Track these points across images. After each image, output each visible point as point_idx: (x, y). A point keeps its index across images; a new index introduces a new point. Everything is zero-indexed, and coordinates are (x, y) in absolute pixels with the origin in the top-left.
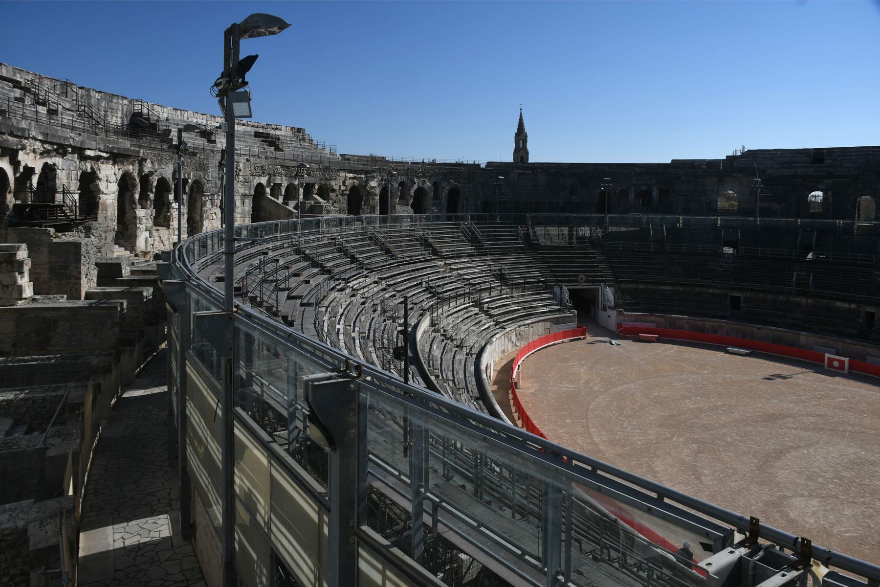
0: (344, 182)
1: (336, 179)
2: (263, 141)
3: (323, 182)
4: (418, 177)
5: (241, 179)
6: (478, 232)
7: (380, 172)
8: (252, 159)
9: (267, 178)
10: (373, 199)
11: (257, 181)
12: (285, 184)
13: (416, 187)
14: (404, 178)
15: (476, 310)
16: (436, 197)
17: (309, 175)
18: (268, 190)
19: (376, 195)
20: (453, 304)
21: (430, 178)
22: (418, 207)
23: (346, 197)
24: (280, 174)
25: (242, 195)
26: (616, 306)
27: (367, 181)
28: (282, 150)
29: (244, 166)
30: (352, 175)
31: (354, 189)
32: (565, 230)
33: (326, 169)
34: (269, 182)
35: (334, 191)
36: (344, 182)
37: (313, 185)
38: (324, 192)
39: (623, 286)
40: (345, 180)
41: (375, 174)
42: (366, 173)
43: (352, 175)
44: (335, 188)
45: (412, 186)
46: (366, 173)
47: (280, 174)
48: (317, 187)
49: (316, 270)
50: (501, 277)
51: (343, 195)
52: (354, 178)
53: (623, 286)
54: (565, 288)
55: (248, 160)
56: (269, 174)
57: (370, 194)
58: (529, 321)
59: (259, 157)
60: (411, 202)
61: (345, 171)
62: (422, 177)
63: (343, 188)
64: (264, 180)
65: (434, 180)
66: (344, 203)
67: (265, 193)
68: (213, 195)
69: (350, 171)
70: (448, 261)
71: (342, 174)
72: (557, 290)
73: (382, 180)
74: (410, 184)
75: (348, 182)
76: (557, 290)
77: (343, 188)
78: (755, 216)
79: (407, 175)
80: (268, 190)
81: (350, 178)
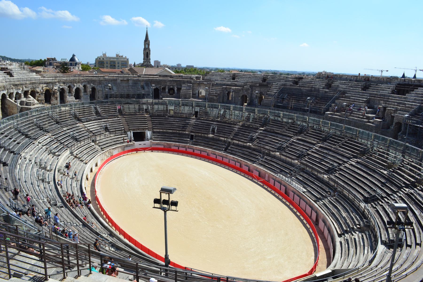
0: (42, 88)
1: (38, 88)
3: (33, 90)
6: (99, 110)
7: (59, 82)
9: (7, 91)
12: (15, 92)
13: (75, 88)
14: (70, 84)
15: (93, 144)
16: (85, 91)
17: (26, 87)
20: (82, 143)
21: (82, 83)
22: (77, 96)
24: (12, 88)
26: (151, 139)
28: (13, 76)
30: (45, 85)
31: (47, 91)
32: (137, 106)
33: (33, 83)
34: (8, 92)
35: (38, 92)
37: (28, 91)
38: (33, 94)
39: (155, 130)
43: (45, 85)
48: (30, 92)
49: (23, 137)
50: (106, 129)
52: (47, 86)
53: (155, 130)
54: (132, 132)
56: (8, 89)
57: (54, 93)
58: (114, 147)
60: (73, 94)
61: (42, 84)
63: (42, 91)
64: (5, 92)
65: (83, 84)
66: (43, 97)
70: (85, 123)
72: (129, 133)
75: (44, 88)
76: (129, 133)
78: (208, 102)
79: (71, 83)
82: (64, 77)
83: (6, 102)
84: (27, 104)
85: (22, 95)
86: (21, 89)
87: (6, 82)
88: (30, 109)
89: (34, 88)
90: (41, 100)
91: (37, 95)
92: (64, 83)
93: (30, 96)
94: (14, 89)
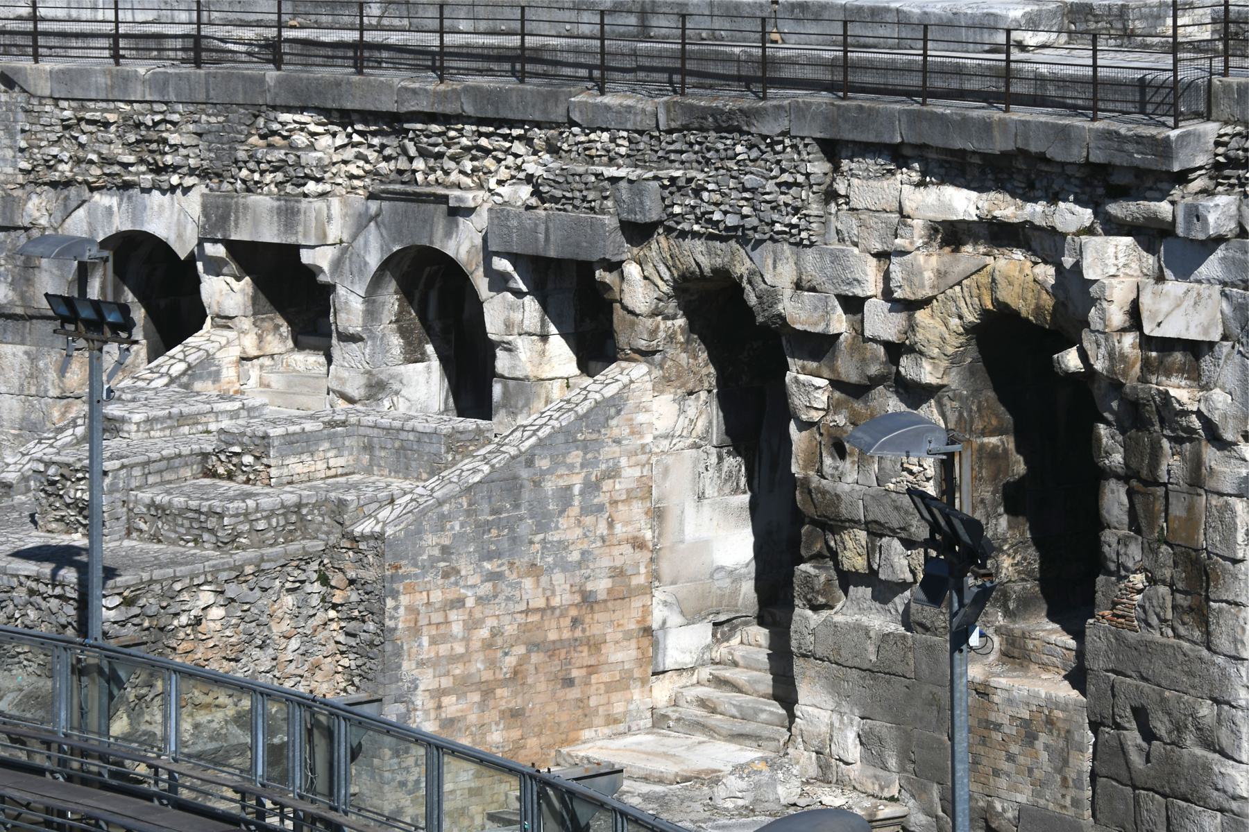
30: (962, 203)
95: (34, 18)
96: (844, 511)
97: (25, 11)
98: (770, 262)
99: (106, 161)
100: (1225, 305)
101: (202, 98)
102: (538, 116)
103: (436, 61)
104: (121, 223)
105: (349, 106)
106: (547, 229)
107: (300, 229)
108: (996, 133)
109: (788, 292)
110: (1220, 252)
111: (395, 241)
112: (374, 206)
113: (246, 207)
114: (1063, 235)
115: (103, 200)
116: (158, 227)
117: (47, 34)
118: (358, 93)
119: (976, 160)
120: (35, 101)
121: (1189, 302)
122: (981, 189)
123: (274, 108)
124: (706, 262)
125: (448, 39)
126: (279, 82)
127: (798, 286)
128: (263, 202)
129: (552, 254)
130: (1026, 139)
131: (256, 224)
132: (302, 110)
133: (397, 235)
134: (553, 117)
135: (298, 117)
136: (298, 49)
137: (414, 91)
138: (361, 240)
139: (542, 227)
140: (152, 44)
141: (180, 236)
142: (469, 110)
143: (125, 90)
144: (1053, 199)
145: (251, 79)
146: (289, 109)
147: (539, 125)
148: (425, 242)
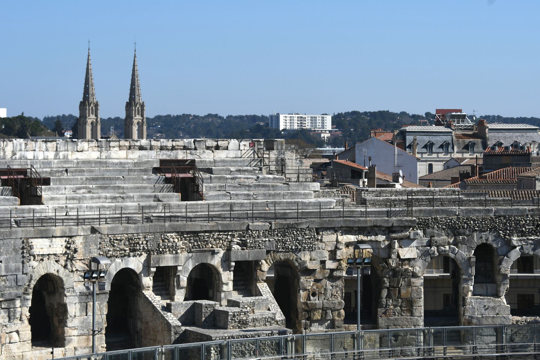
0: (333, 255)
1: (311, 249)
2: (167, 181)
3: (281, 256)
4: (523, 234)
5: (79, 265)
7: (424, 225)
8: (104, 228)
10: (409, 284)
11: (114, 267)
13: (515, 255)
14: (489, 237)
17: (243, 244)
18: (147, 281)
19: (414, 275)
23: (340, 283)
24: (174, 249)
25: (82, 294)
27: (390, 247)
29: (86, 244)
30: (352, 238)
33: (285, 230)
34: (147, 265)
35: (310, 272)
36: (333, 255)
37: (257, 264)
40: (337, 248)
41: (410, 233)
42: (389, 231)
44: (310, 265)
45: (506, 254)
46: (389, 231)
47: (174, 249)
51: (332, 278)
55: (94, 231)
56: (149, 252)
59: (129, 220)
61: (335, 230)
62: (531, 233)
63: (330, 265)
64: (135, 263)
67: (139, 287)
68: (12, 300)
69: (348, 230)
71: (329, 238)
73: (430, 244)
74: (505, 249)
75: (344, 253)
77: (330, 265)
79: (493, 229)
80: (147, 281)
81: (348, 245)
82: (460, 202)
83: (141, 306)
84: (217, 320)
85: (227, 277)
86: (222, 252)
87: (148, 220)
88: (209, 338)
89: (287, 250)
90: (324, 310)
91: (307, 282)
92: (454, 230)
93: (263, 287)
94: (183, 255)
95: (78, 215)
96: (317, 307)
97: (76, 213)
98: (303, 255)
99: (122, 250)
100: (418, 251)
101: (148, 231)
102: (238, 229)
103: (209, 218)
104: (123, 266)
105: (187, 230)
106: (249, 254)
107: (179, 261)
108: (368, 222)
109: (308, 261)
110: (416, 241)
111: (196, 262)
112: (190, 255)
113: (164, 258)
114: (380, 242)
115: (118, 260)
116: (132, 266)
117: (58, 219)
118: (190, 227)
119: (356, 229)
120: (103, 236)
121: (410, 251)
122: (355, 235)
123: (165, 232)
124: (282, 258)
125: (188, 214)
126: (169, 226)
127: (311, 260)
128: (168, 255)
129: (251, 259)
130: (377, 223)
131: (167, 261)
132: (173, 232)
133: (197, 260)
134: (243, 229)
135: (171, 234)
136: (157, 218)
137: (206, 225)
138: (187, 263)
139: (247, 254)
140: (117, 219)
141: (138, 268)
142: (220, 229)
143: (127, 231)
144: (376, 235)
145: (162, 226)
146: (169, 233)
147: (236, 231)
148: (205, 262)
